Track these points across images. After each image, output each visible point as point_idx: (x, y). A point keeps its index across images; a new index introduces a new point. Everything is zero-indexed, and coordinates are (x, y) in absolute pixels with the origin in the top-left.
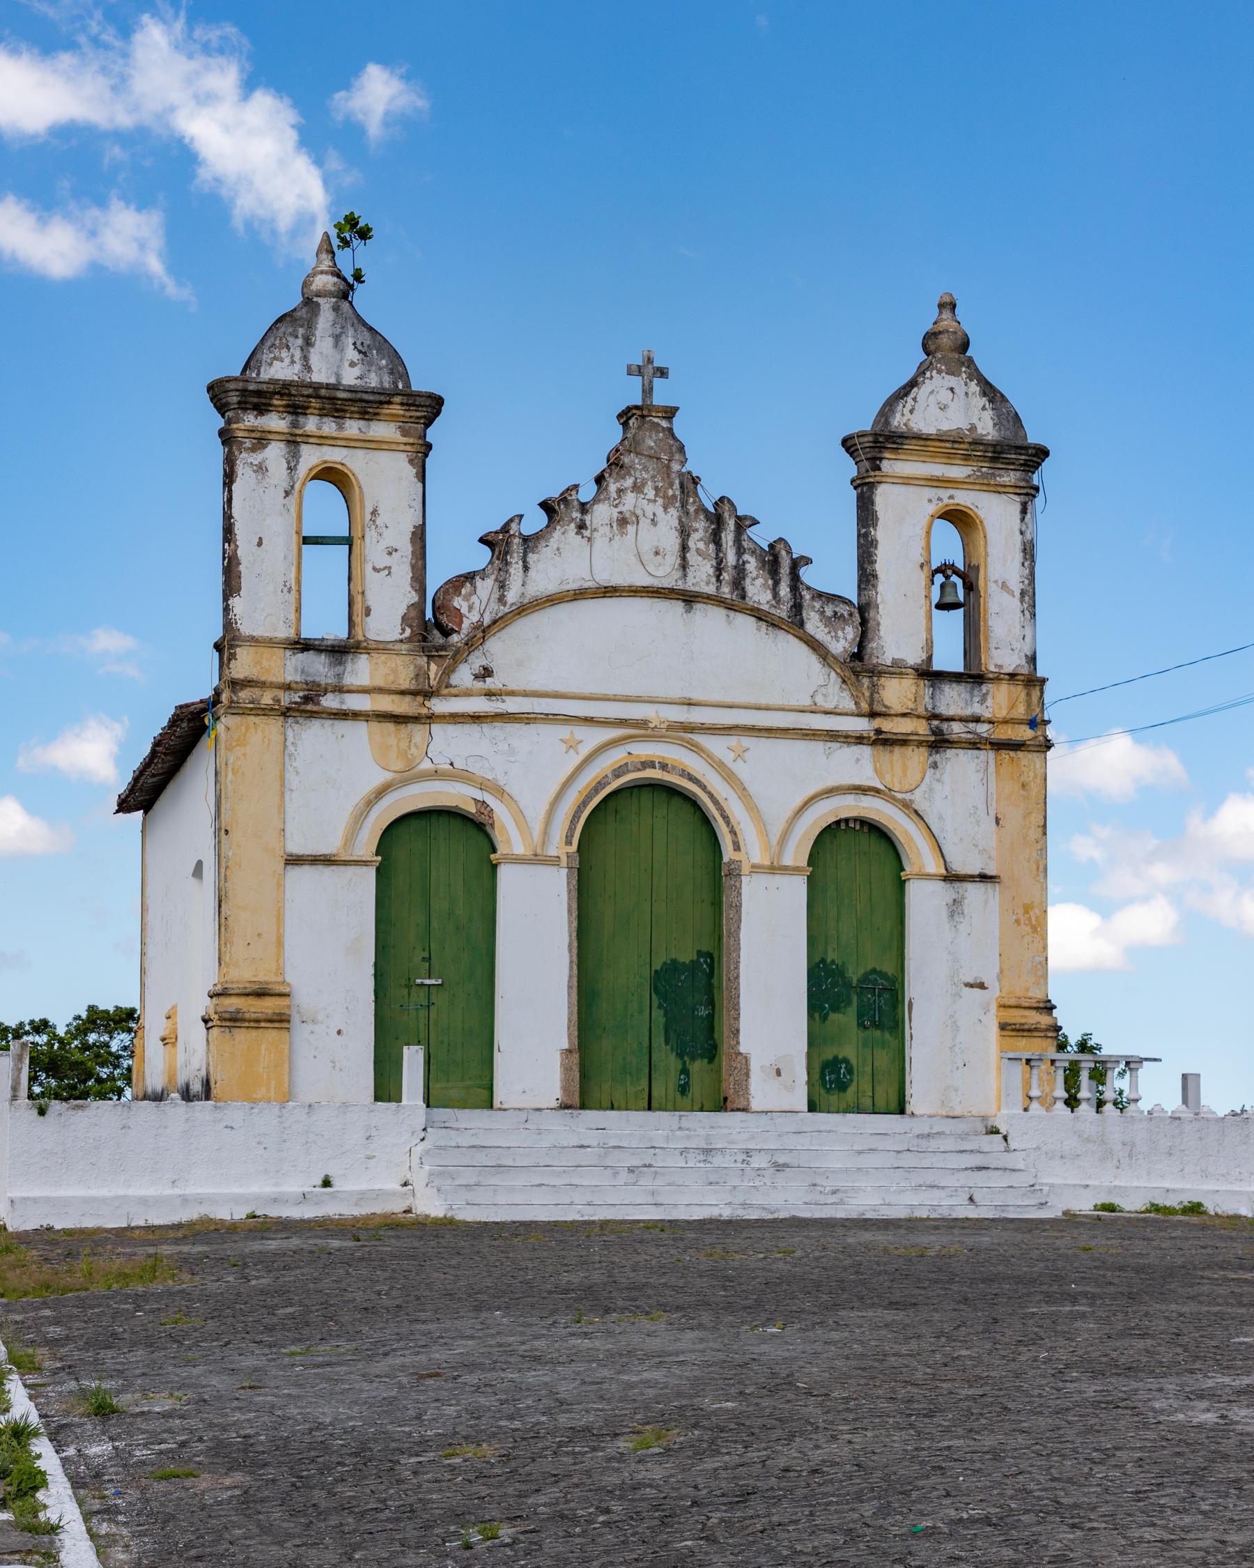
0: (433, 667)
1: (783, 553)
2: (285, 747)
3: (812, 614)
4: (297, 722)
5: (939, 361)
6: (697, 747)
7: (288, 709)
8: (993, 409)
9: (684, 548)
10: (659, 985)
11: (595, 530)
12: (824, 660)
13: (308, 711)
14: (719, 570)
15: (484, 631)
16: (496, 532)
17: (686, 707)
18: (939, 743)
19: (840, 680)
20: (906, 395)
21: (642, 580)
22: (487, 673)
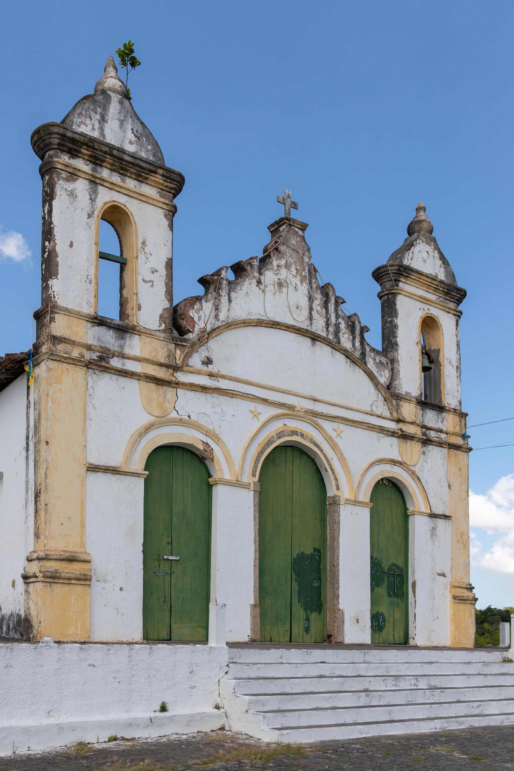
0: (178, 352)
1: (357, 322)
2: (87, 389)
3: (370, 359)
4: (95, 373)
5: (423, 235)
6: (319, 426)
7: (90, 363)
8: (444, 268)
9: (311, 309)
11: (266, 286)
12: (376, 386)
13: (103, 366)
14: (328, 325)
15: (208, 334)
16: (213, 275)
17: (313, 402)
18: (426, 442)
19: (383, 399)
20: (409, 249)
21: (290, 321)
22: (208, 362)
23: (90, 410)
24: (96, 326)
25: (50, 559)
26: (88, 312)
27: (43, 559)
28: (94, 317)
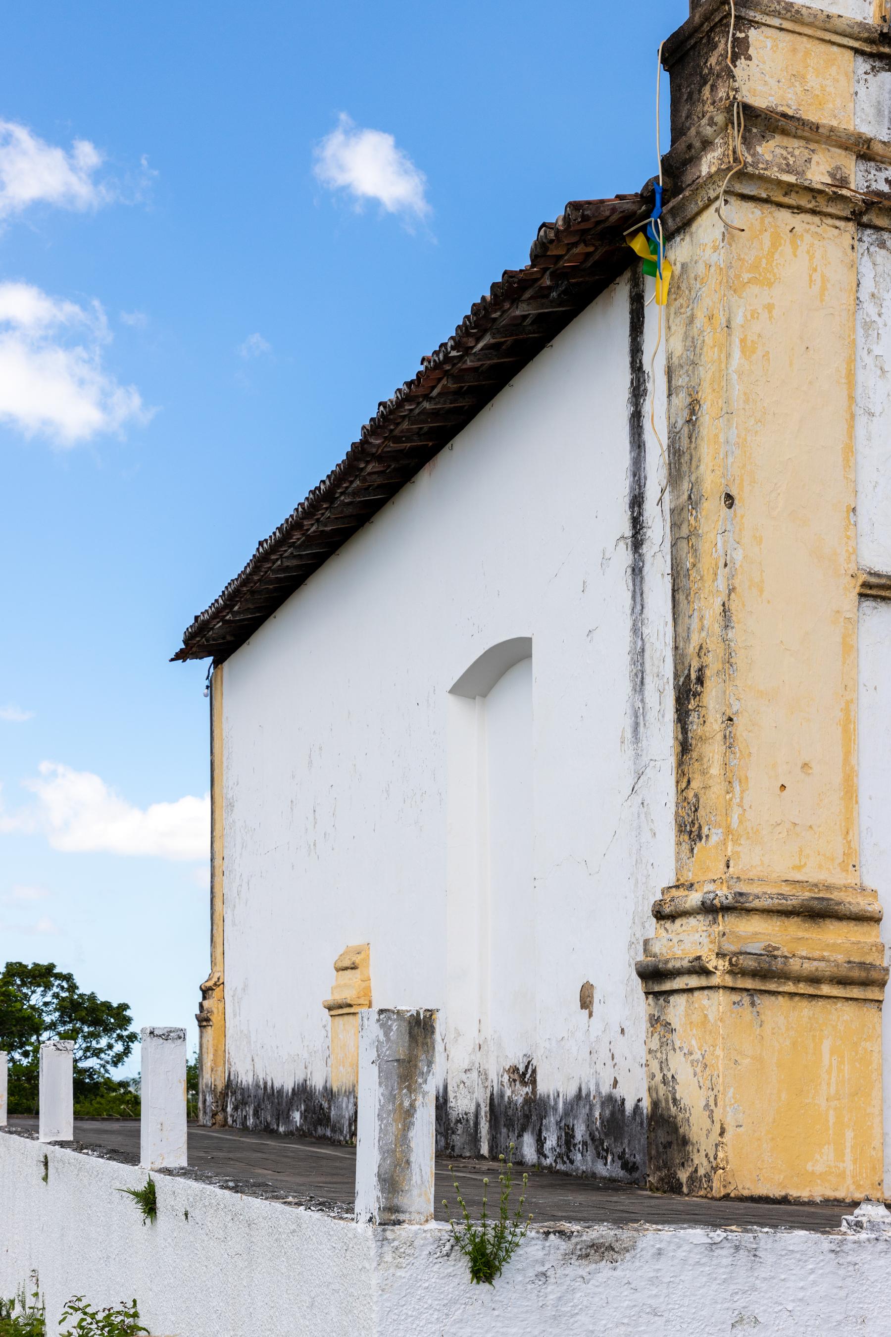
23: (867, 377)
24: (883, 69)
25: (749, 911)
26: (859, 19)
27: (726, 909)
28: (882, 34)
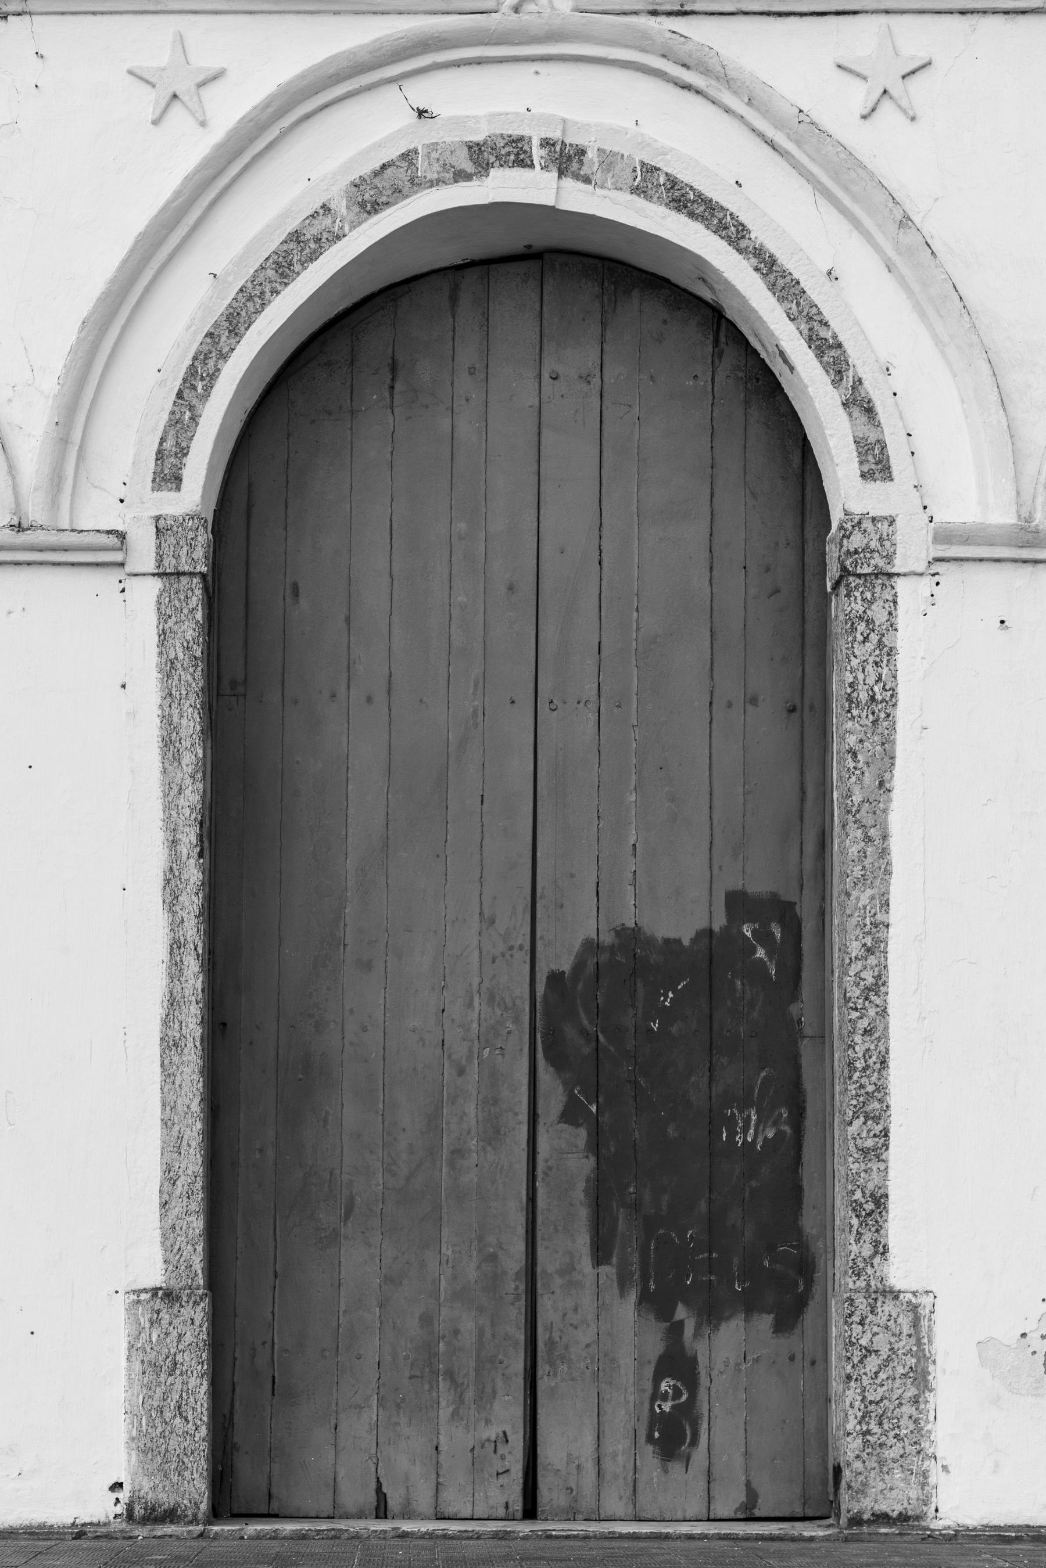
10: (570, 1032)
